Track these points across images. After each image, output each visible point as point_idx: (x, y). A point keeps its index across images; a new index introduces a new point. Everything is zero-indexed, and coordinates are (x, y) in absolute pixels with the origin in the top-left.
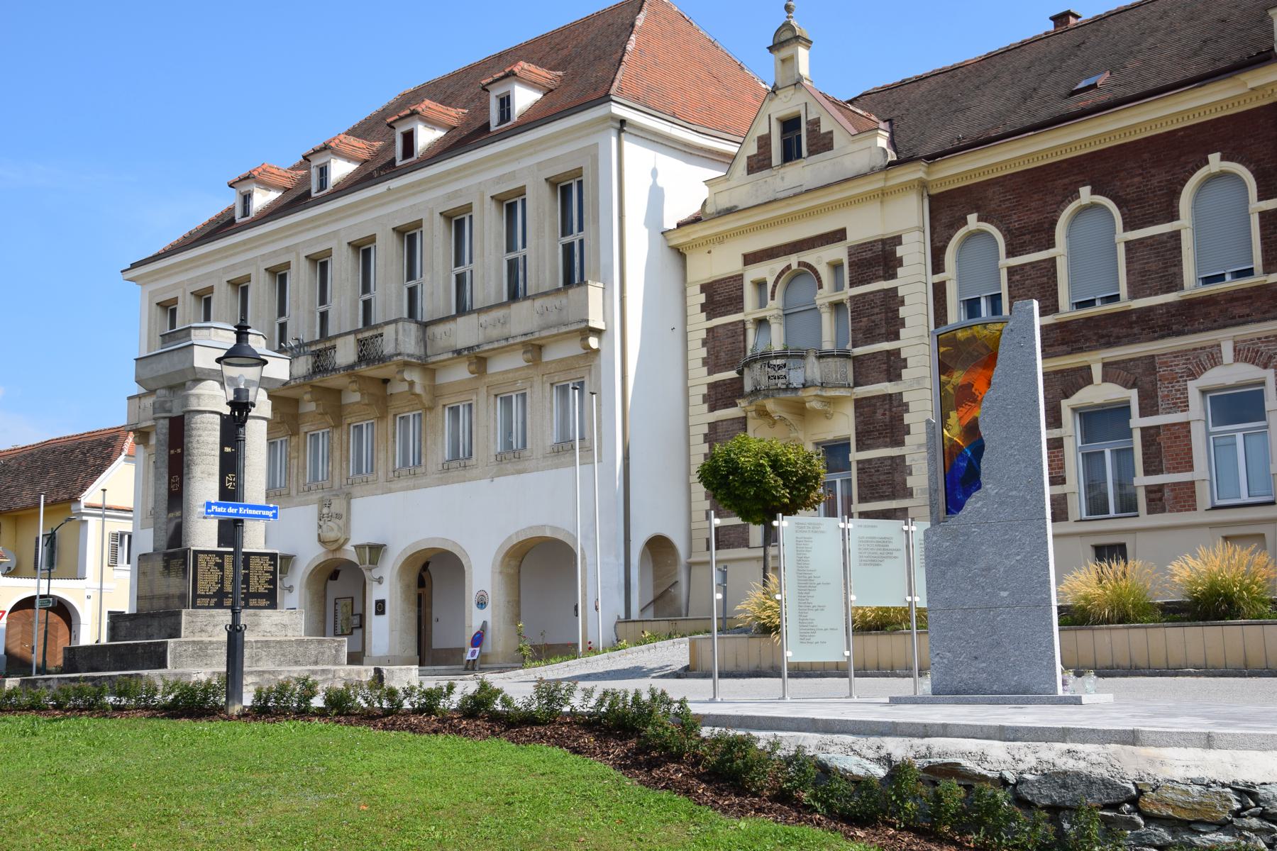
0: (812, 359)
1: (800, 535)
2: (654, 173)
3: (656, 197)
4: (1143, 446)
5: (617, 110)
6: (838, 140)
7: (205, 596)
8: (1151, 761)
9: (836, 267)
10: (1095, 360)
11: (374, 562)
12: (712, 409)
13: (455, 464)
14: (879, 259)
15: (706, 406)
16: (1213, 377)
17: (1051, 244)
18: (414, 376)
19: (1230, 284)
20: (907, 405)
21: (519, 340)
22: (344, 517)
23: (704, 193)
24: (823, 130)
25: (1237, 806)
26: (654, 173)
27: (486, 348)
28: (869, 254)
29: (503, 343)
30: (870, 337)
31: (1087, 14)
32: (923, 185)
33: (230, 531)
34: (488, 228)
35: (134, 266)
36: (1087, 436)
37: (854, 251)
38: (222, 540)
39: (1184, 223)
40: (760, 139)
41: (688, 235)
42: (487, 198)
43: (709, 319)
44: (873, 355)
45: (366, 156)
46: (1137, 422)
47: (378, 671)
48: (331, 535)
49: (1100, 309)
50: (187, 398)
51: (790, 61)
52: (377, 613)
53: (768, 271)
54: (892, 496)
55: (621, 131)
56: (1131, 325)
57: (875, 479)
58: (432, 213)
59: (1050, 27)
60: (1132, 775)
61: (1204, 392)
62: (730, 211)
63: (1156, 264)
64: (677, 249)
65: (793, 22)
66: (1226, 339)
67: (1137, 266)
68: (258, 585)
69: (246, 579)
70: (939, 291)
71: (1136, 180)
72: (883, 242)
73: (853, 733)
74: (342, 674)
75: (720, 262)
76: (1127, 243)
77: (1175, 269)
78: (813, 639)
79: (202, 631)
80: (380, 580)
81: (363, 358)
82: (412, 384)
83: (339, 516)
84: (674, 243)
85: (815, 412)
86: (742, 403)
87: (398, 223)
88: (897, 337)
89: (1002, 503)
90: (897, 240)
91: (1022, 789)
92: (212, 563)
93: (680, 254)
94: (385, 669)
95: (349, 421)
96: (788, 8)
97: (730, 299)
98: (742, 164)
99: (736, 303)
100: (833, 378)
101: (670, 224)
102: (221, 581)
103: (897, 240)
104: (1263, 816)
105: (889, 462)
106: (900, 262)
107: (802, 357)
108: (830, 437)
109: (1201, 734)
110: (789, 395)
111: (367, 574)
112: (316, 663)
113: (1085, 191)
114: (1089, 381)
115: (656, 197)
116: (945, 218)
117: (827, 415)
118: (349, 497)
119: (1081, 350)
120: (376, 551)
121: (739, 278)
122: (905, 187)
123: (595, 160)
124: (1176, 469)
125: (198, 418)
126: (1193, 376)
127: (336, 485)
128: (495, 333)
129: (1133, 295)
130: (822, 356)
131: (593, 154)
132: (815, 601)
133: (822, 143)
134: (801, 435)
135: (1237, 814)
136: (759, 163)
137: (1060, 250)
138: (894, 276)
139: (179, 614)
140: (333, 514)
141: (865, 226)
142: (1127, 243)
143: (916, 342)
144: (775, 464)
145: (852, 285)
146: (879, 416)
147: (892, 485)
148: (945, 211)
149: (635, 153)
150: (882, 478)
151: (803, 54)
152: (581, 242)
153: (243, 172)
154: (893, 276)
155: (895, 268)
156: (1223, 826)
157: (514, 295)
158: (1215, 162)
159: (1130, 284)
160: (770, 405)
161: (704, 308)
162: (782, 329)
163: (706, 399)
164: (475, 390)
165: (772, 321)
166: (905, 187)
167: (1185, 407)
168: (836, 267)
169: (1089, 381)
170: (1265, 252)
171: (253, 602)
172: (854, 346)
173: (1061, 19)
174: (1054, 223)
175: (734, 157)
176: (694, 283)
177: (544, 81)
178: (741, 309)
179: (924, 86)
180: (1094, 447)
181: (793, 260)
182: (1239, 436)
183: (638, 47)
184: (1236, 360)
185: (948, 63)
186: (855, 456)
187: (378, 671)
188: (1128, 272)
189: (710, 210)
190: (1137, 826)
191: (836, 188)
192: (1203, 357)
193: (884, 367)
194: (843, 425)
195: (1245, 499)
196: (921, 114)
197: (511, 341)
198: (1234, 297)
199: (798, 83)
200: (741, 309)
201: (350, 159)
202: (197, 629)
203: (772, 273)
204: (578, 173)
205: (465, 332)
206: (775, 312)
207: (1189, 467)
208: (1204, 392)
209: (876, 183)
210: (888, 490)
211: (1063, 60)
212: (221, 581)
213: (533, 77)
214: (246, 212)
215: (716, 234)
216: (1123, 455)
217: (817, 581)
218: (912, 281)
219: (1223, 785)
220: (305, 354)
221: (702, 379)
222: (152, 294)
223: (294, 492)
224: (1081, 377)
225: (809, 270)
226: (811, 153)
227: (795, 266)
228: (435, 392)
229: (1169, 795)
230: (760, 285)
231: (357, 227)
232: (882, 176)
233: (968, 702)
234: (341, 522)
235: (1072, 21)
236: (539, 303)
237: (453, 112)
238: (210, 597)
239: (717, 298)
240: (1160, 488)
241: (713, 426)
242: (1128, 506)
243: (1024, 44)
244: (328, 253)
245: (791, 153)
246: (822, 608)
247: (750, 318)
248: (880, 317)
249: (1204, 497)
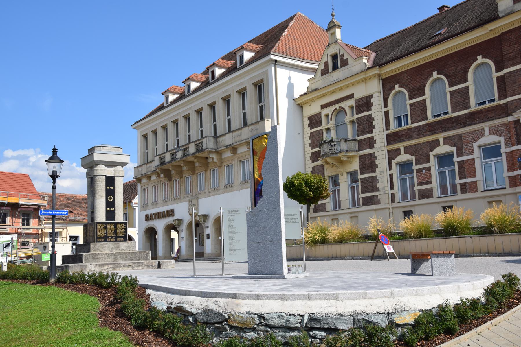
0: (342, 142)
1: (229, 215)
2: (290, 78)
3: (291, 87)
4: (459, 168)
5: (272, 57)
6: (350, 61)
7: (100, 238)
8: (237, 305)
9: (352, 107)
10: (441, 137)
11: (205, 221)
12: (313, 162)
13: (228, 186)
14: (365, 104)
16: (482, 141)
17: (424, 94)
18: (213, 156)
19: (488, 105)
20: (376, 157)
21: (245, 141)
22: (196, 206)
23: (307, 84)
24: (345, 58)
25: (257, 322)
26: (290, 78)
27: (235, 144)
28: (362, 102)
29: (240, 143)
30: (363, 133)
31: (451, 6)
32: (379, 75)
33: (110, 215)
34: (235, 101)
35: (135, 123)
36: (440, 165)
37: (357, 101)
38: (107, 218)
39: (470, 83)
40: (325, 63)
41: (302, 100)
42: (235, 92)
44: (365, 139)
45: (204, 80)
46: (456, 159)
47: (159, 262)
49: (442, 117)
50: (93, 171)
51: (333, 34)
53: (329, 111)
54: (373, 191)
55: (275, 64)
56: (453, 123)
57: (366, 185)
59: (438, 12)
60: (228, 311)
61: (480, 147)
62: (316, 90)
63: (461, 99)
64: (299, 104)
65: (334, 20)
66: (486, 126)
67: (454, 100)
68: (120, 233)
69: (115, 232)
70: (387, 114)
71: (453, 68)
72: (367, 97)
74: (145, 264)
75: (313, 109)
76: (450, 92)
77: (467, 101)
78: (235, 253)
79: (98, 250)
80: (208, 227)
81: (197, 151)
82: (213, 158)
84: (298, 103)
85: (346, 162)
86: (320, 159)
87: (209, 103)
88: (372, 132)
89: (268, 203)
90: (371, 96)
91: (197, 316)
92: (102, 227)
93: (301, 106)
94: (161, 261)
96: (332, 15)
97: (317, 122)
98: (319, 72)
99: (319, 123)
100: (352, 148)
101: (296, 95)
102: (106, 232)
103: (371, 96)
104: (267, 325)
105: (371, 179)
107: (339, 141)
108: (351, 170)
109: (256, 294)
110: (334, 156)
111: (203, 225)
112: (139, 260)
113: (435, 74)
114: (439, 145)
115: (291, 87)
116: (388, 87)
117: (350, 162)
118: (197, 199)
119: (436, 133)
121: (320, 114)
122: (372, 77)
123: (267, 75)
124: (470, 177)
125: (97, 177)
126: (475, 141)
127: (194, 195)
128: (237, 139)
129: (453, 111)
130: (346, 141)
131: (267, 73)
132: (235, 239)
133: (345, 63)
134: (342, 170)
135: (258, 325)
136: (325, 72)
137: (427, 96)
139: (90, 245)
140: (193, 205)
141: (360, 92)
142: (450, 92)
143: (379, 134)
144: (306, 183)
145: (357, 114)
146: (367, 162)
147: (372, 187)
148: (388, 84)
149: (281, 71)
150: (369, 184)
151: (338, 32)
153: (166, 90)
154: (370, 110)
155: (370, 107)
156: (254, 330)
157: (245, 124)
158: (480, 59)
159: (452, 107)
160: (328, 160)
161: (309, 125)
162: (335, 132)
163: (311, 158)
164: (233, 159)
165: (331, 129)
166: (372, 77)
167: (473, 153)
168: (352, 107)
169: (439, 145)
170: (499, 92)
171: (118, 239)
172: (358, 136)
173: (441, 9)
174: (425, 86)
175: (316, 70)
176: (306, 117)
177: (255, 49)
178: (321, 125)
179: (393, 38)
180: (442, 170)
181: (337, 106)
182: (493, 163)
183: (288, 34)
184: (490, 134)
185: (402, 29)
186: (360, 177)
187: (159, 262)
188: (451, 103)
189: (309, 90)
190: (227, 330)
191: (349, 79)
192: (478, 134)
193: (368, 143)
194: (355, 166)
195: (495, 187)
196: (386, 50)
197: (242, 142)
198: (488, 110)
199: (336, 42)
200: (321, 125)
201: (197, 82)
202: (96, 249)
203: (330, 111)
204: (262, 81)
205: (228, 139)
206: (332, 125)
207: (475, 176)
208: (480, 147)
209: (362, 76)
210: (371, 189)
211: (436, 24)
212: (106, 232)
213: (251, 48)
214: (167, 103)
215: (311, 99)
216: (452, 172)
217: (236, 231)
218: (377, 112)
219: (255, 314)
221: (309, 151)
222: (141, 132)
223: (182, 198)
225: (342, 109)
226: (341, 67)
227: (338, 109)
228: (221, 161)
229: (237, 318)
230: (327, 116)
231: (196, 105)
232: (363, 73)
233: (267, 278)
234: (195, 207)
235: (446, 9)
236: (250, 127)
237: (229, 62)
238: (102, 238)
239: (313, 122)
240: (465, 184)
241: (313, 168)
242: (454, 192)
243: (428, 19)
244: (189, 114)
245: (335, 67)
246: (239, 241)
247: (324, 128)
248: (366, 125)
249: (481, 187)
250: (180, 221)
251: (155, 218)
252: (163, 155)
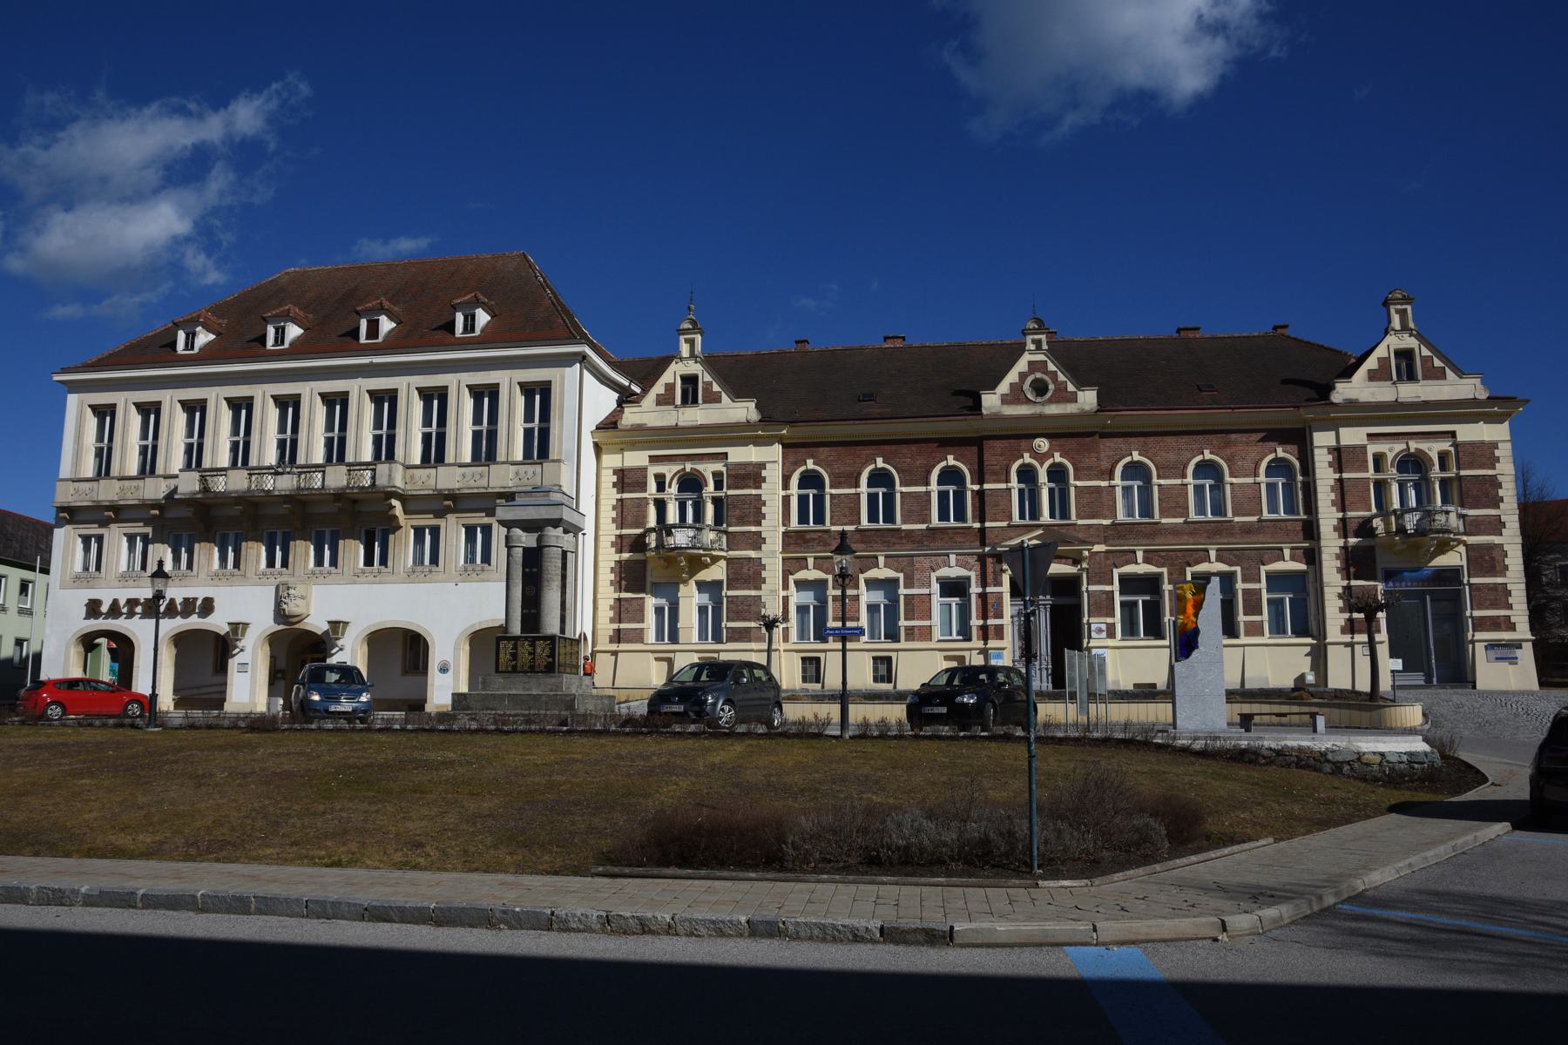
73: (1053, 738)
103: (762, 466)
106: (764, 480)
121: (645, 469)
129: (904, 522)
138: (759, 487)
141: (740, 455)
174: (859, 474)
218: (772, 492)
224: (802, 563)
240: (913, 628)
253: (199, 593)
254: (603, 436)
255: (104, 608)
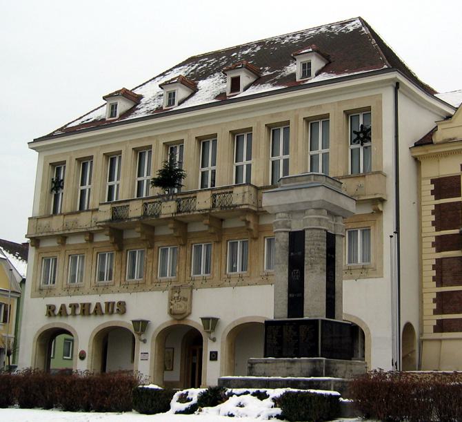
15: (434, 249)
22: (188, 300)
42: (301, 119)
43: (436, 199)
48: (180, 310)
52: (211, 359)
58: (259, 124)
82: (248, 223)
83: (185, 299)
87: (234, 128)
95: (193, 242)
118: (192, 288)
120: (211, 323)
123: (380, 103)
140: (180, 296)
152: (214, 172)
163: (434, 245)
176: (427, 178)
220: (172, 200)
241: (439, 261)
250: (142, 325)
251: (74, 314)
252: (125, 204)
253: (116, 298)
254: (419, 152)
255: (57, 312)
